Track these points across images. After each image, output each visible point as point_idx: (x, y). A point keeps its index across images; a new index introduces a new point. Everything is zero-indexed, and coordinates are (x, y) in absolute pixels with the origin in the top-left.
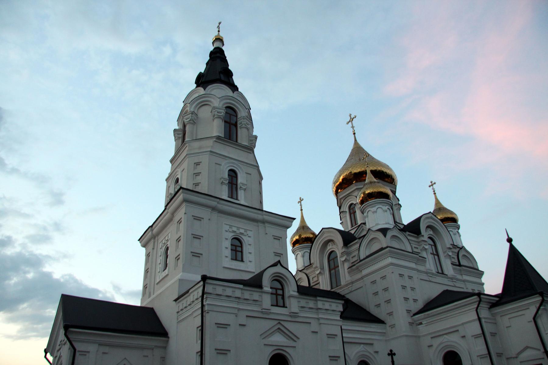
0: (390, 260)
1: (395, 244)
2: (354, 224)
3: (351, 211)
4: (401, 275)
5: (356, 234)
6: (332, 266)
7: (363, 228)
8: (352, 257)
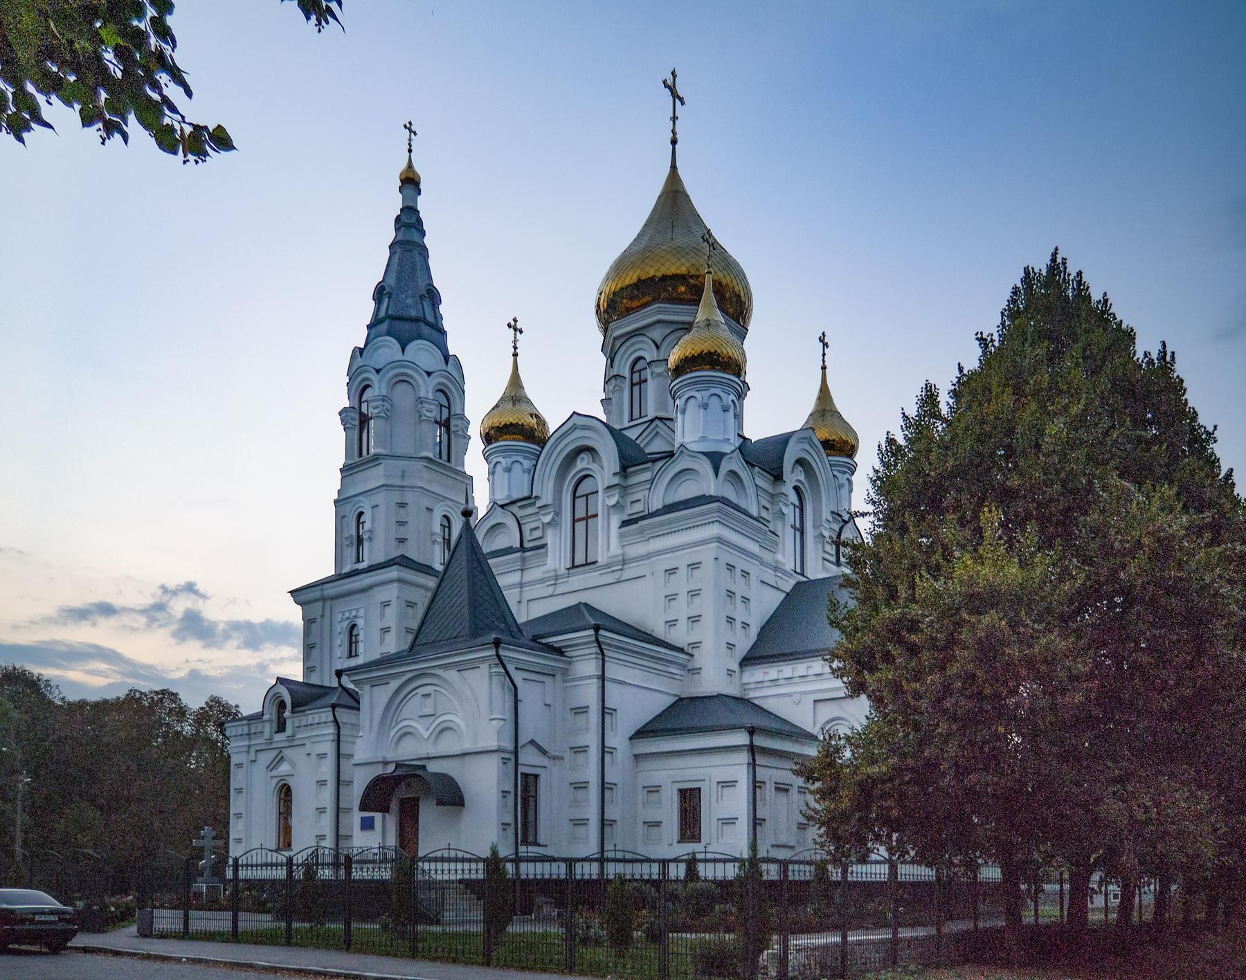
0: (715, 530)
1: (730, 493)
2: (636, 414)
3: (636, 377)
4: (731, 567)
5: (641, 442)
6: (580, 513)
7: (658, 430)
8: (632, 503)
